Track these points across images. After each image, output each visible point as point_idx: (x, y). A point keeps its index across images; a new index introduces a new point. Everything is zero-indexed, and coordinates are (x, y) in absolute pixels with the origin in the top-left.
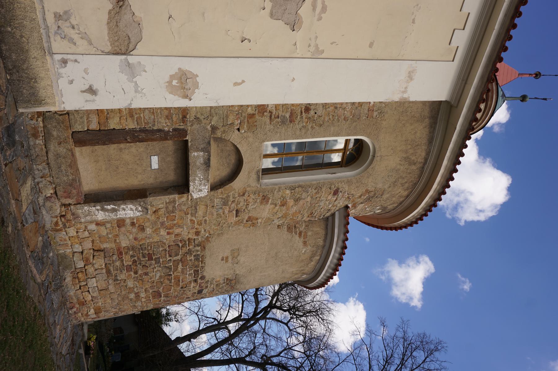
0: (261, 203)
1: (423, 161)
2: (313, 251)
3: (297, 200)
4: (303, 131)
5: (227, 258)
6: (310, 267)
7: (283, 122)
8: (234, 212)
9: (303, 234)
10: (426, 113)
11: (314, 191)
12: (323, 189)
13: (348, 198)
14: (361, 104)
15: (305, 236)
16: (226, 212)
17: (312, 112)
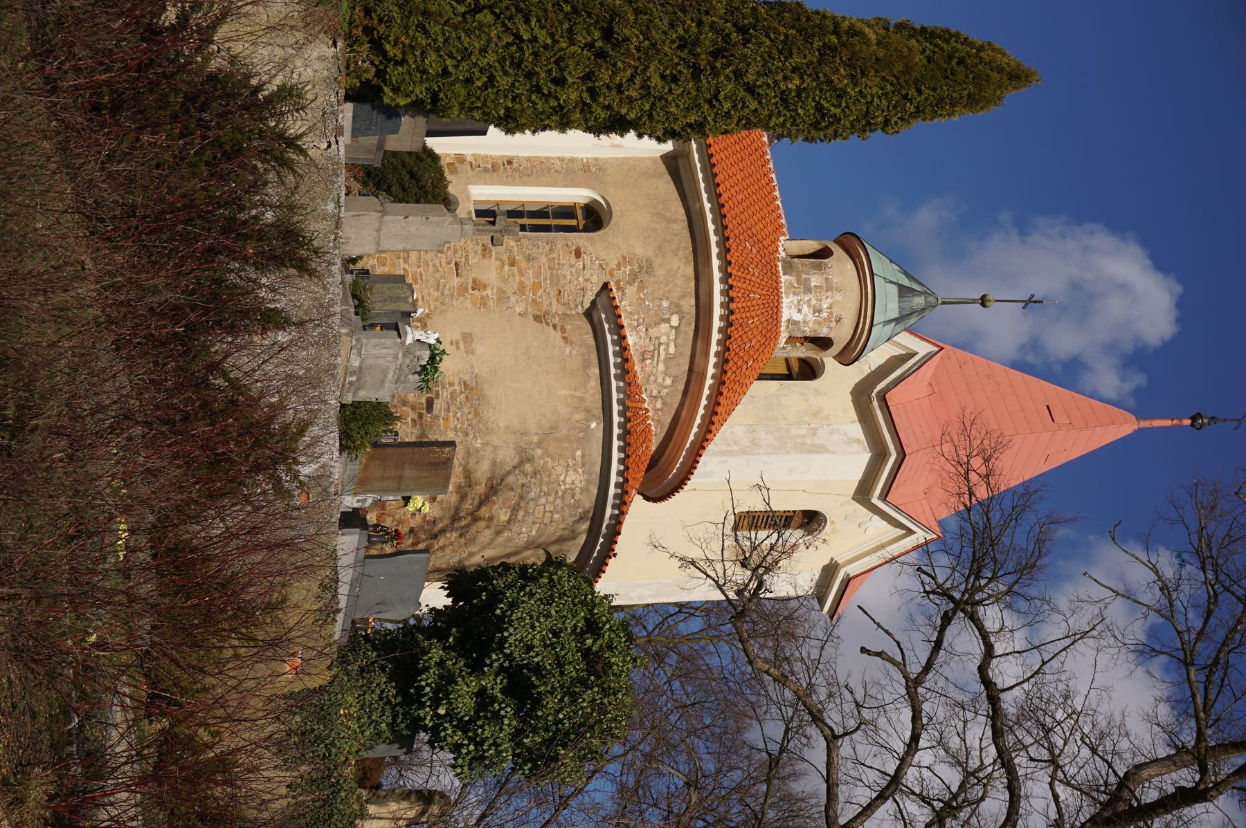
0: (484, 256)
1: (685, 218)
2: (583, 355)
3: (529, 258)
4: (511, 179)
5: (457, 342)
6: (592, 392)
7: (486, 170)
8: (453, 265)
9: (559, 328)
10: (662, 168)
11: (548, 247)
12: (559, 246)
13: (601, 265)
14: (572, 160)
15: (563, 330)
16: (444, 264)
17: (515, 165)
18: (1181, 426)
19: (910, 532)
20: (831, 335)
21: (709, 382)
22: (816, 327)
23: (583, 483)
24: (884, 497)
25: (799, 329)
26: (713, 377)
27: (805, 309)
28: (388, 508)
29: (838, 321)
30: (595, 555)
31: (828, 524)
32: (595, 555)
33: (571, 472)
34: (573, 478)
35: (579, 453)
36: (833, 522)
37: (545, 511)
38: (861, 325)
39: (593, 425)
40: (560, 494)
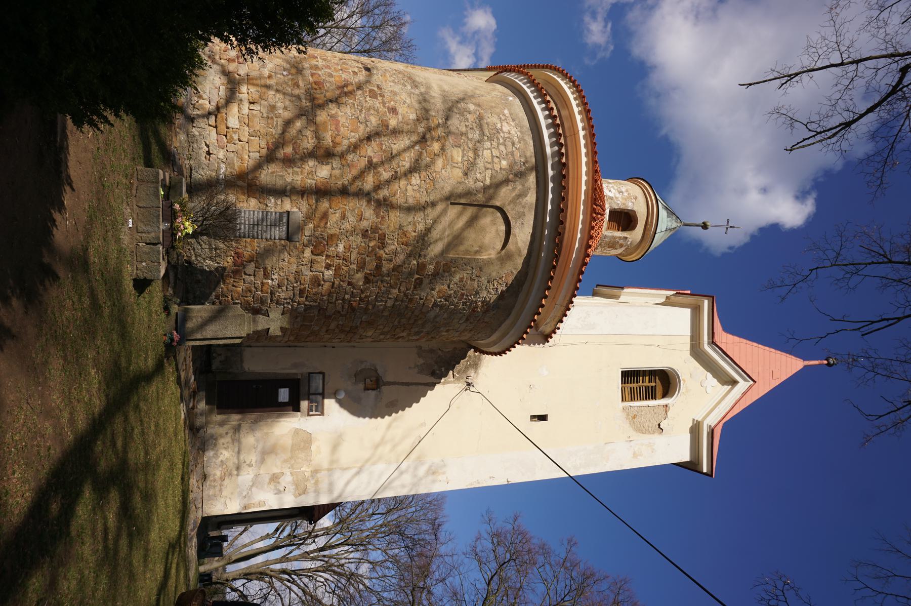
18: (823, 364)
19: (734, 383)
20: (635, 209)
21: (582, 133)
22: (624, 201)
23: (519, 133)
24: (712, 342)
25: (615, 202)
26: (583, 129)
27: (612, 189)
28: (342, 129)
29: (636, 198)
30: (549, 207)
31: (682, 382)
32: (549, 207)
33: (505, 124)
34: (508, 128)
35: (506, 112)
36: (684, 381)
37: (493, 156)
38: (650, 202)
39: (511, 98)
40: (501, 141)
